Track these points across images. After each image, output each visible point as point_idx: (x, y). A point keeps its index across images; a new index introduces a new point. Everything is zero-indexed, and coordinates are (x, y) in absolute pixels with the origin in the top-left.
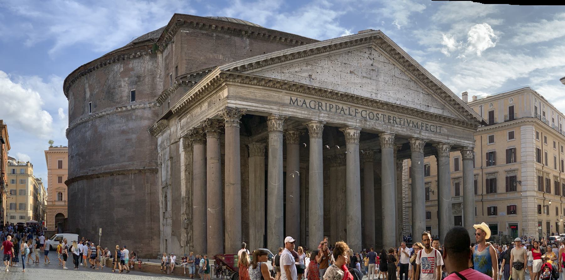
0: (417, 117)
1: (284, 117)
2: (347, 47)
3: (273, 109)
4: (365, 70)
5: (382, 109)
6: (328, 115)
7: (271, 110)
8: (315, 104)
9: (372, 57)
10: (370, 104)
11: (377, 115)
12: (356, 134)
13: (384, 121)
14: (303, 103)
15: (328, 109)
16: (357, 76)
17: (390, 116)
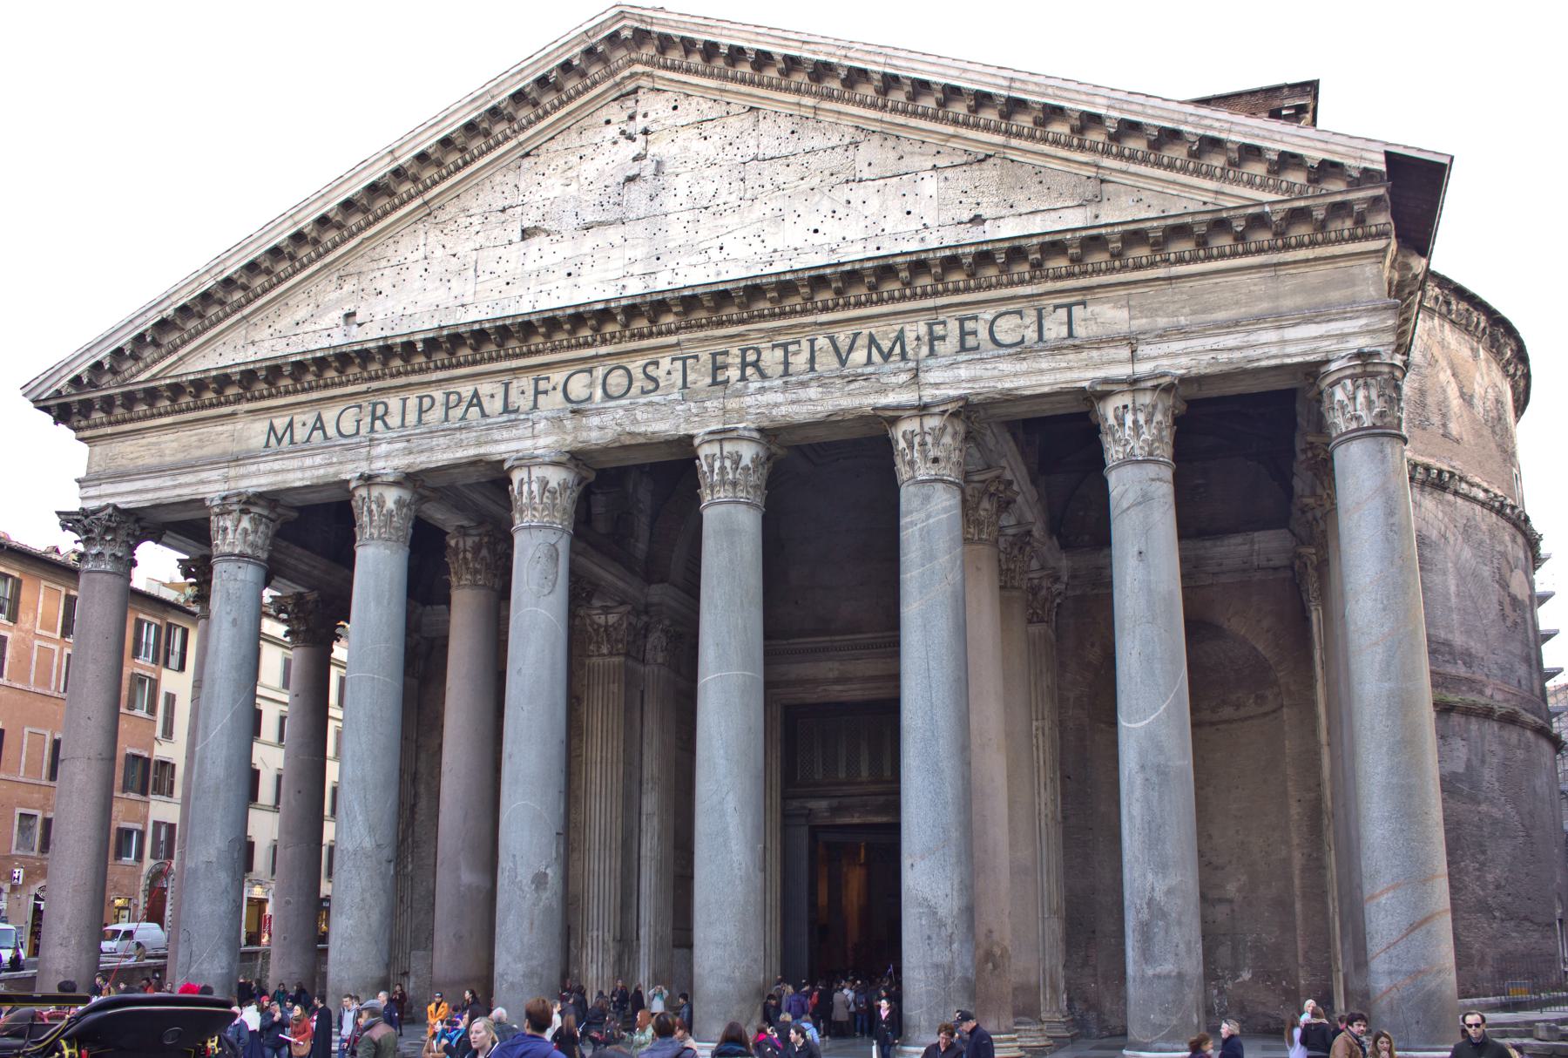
0: (881, 301)
1: (235, 499)
2: (498, 144)
3: (209, 482)
4: (594, 198)
5: (660, 334)
6: (405, 444)
7: (202, 489)
8: (361, 416)
9: (640, 123)
10: (585, 333)
11: (650, 369)
12: (525, 488)
13: (685, 385)
14: (314, 428)
15: (412, 418)
16: (558, 237)
17: (726, 353)
